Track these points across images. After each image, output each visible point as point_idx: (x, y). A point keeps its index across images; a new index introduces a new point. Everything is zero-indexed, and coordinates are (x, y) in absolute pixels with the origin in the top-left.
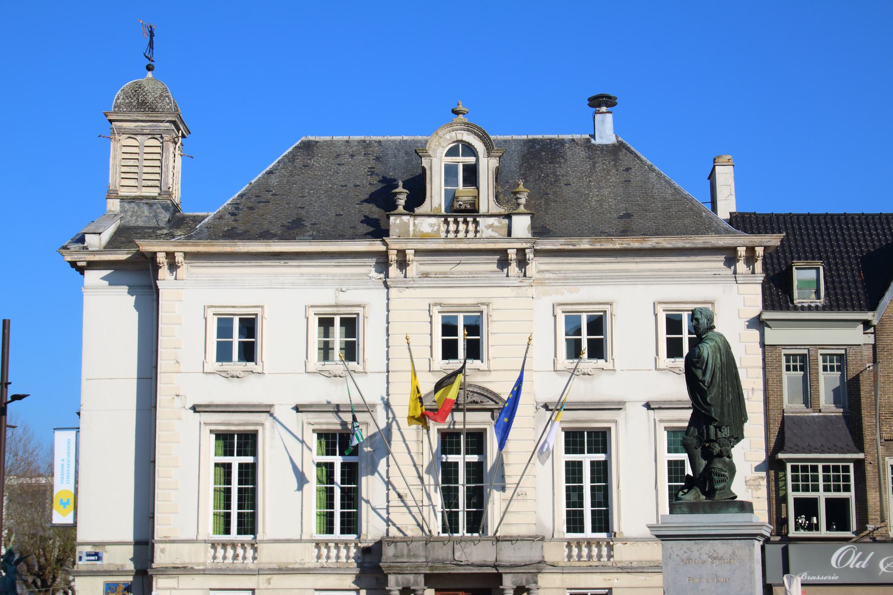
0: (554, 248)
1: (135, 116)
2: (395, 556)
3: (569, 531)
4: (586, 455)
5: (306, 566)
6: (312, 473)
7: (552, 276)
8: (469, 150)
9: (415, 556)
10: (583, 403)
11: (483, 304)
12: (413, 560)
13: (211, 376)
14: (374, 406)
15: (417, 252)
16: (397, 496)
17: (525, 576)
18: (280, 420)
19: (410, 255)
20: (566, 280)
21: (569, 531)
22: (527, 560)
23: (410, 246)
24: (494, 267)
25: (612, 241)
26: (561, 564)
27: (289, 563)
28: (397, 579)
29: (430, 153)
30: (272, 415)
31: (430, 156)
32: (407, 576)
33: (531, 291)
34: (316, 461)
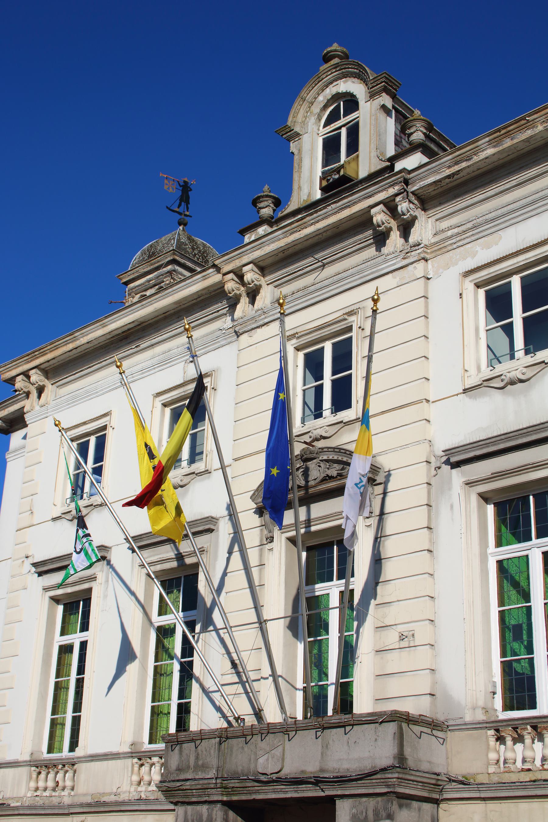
0: (438, 177)
1: (142, 270)
2: (179, 770)
3: (508, 706)
4: (534, 541)
5: (121, 798)
6: (146, 646)
7: (456, 230)
8: (351, 103)
9: (204, 767)
10: (507, 436)
11: (351, 313)
12: (200, 775)
13: (58, 522)
14: (212, 520)
15: (263, 268)
16: (230, 664)
17: (371, 803)
18: (117, 568)
19: (251, 275)
20: (477, 230)
21: (508, 706)
22: (367, 766)
23: (246, 259)
24: (372, 251)
25: (531, 125)
26: (482, 779)
27: (104, 794)
28: (186, 813)
29: (297, 129)
30: (109, 563)
31: (298, 135)
32: (198, 808)
33: (419, 269)
34: (156, 625)
